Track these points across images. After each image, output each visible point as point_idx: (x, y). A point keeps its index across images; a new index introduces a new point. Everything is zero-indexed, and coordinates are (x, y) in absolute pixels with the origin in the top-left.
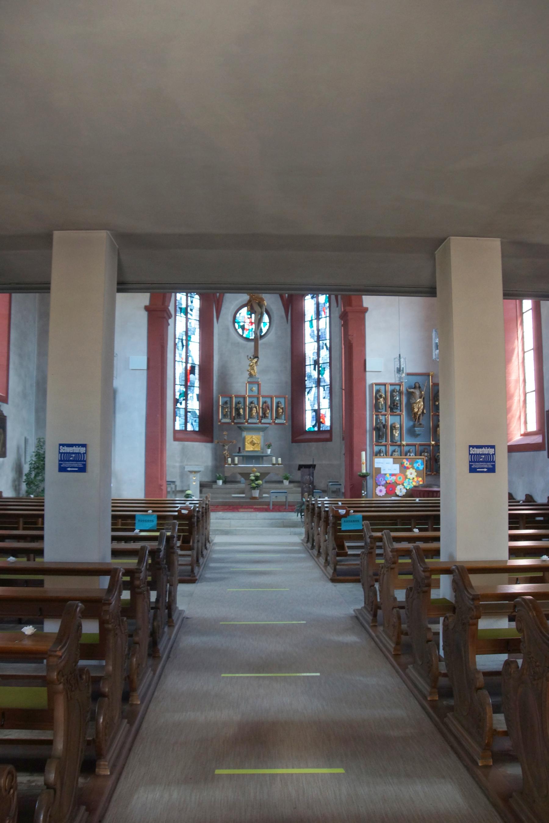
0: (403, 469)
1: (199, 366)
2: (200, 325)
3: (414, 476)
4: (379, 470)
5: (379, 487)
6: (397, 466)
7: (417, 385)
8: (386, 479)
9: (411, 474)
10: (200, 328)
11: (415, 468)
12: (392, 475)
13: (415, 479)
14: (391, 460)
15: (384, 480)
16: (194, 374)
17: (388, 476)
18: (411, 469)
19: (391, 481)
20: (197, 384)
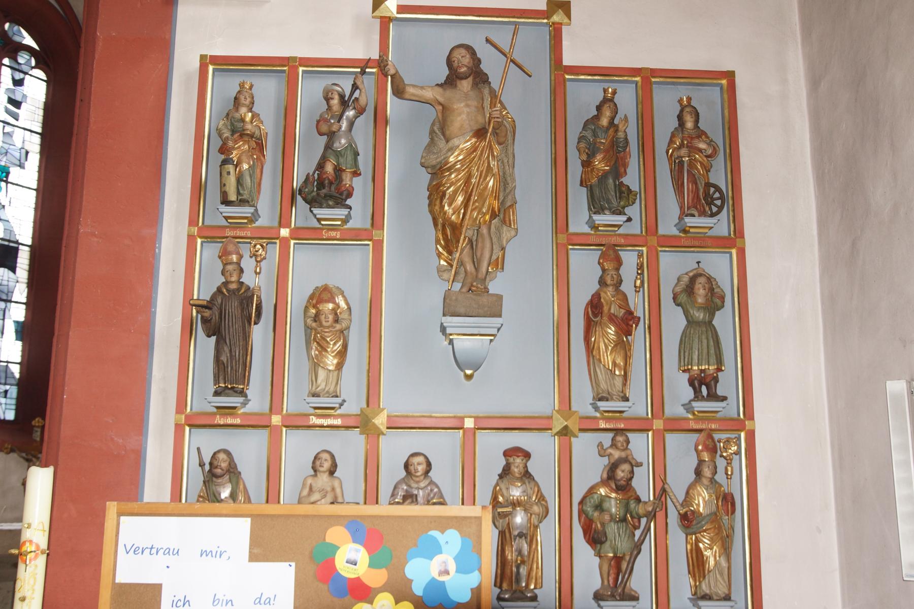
1: (35, 250)
2: (43, 145)
7: (463, 60)
10: (42, 152)
14: (235, 531)
16: (13, 269)
20: (21, 293)
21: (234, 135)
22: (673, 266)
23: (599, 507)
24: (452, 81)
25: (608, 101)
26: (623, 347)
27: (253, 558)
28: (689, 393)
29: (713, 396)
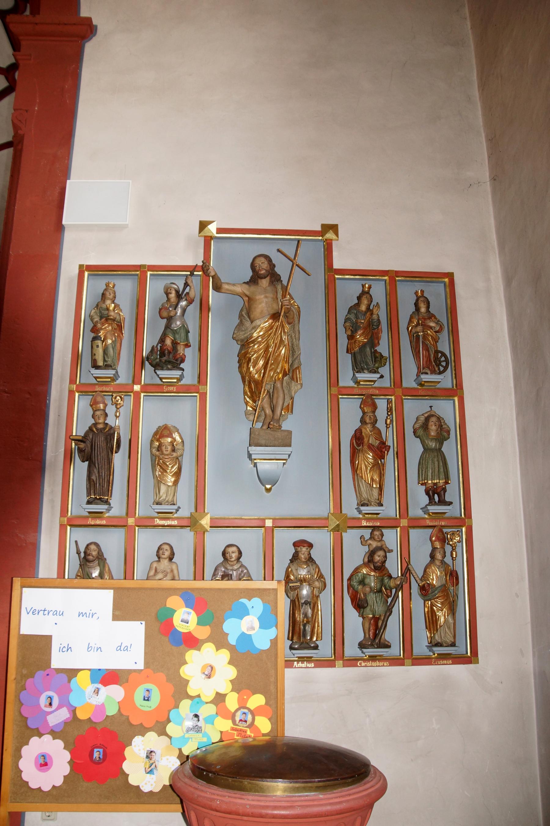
0: (168, 644)
3: (225, 687)
4: (41, 645)
5: (34, 740)
6: (135, 632)
7: (263, 265)
8: (74, 699)
9: (208, 671)
11: (232, 640)
12: (110, 677)
13: (232, 702)
14: (102, 599)
15: (65, 703)
17: (83, 681)
18: (209, 648)
19: (101, 708)
21: (103, 317)
22: (414, 409)
23: (362, 582)
24: (255, 279)
25: (365, 293)
26: (379, 467)
27: (115, 618)
28: (425, 500)
29: (442, 502)
